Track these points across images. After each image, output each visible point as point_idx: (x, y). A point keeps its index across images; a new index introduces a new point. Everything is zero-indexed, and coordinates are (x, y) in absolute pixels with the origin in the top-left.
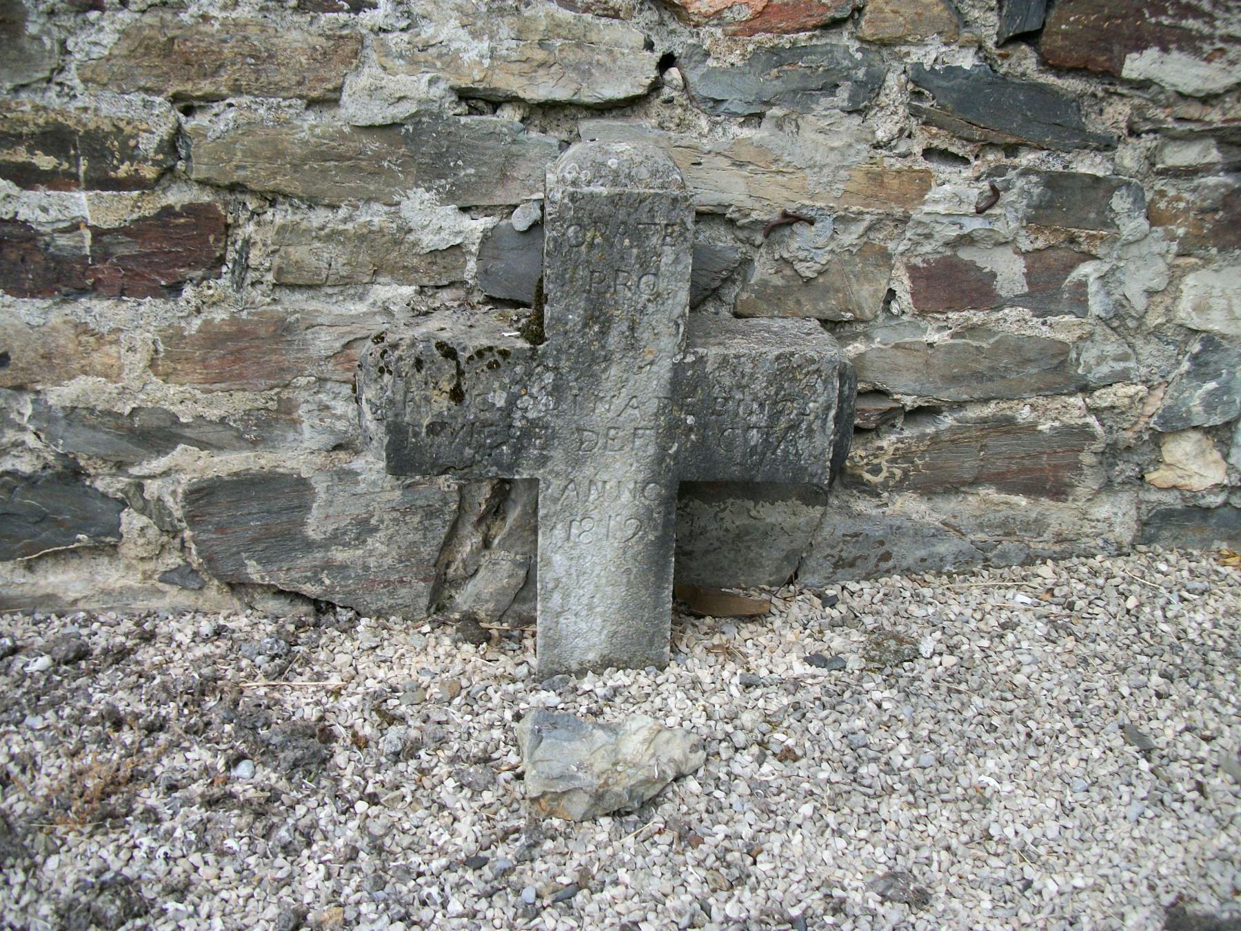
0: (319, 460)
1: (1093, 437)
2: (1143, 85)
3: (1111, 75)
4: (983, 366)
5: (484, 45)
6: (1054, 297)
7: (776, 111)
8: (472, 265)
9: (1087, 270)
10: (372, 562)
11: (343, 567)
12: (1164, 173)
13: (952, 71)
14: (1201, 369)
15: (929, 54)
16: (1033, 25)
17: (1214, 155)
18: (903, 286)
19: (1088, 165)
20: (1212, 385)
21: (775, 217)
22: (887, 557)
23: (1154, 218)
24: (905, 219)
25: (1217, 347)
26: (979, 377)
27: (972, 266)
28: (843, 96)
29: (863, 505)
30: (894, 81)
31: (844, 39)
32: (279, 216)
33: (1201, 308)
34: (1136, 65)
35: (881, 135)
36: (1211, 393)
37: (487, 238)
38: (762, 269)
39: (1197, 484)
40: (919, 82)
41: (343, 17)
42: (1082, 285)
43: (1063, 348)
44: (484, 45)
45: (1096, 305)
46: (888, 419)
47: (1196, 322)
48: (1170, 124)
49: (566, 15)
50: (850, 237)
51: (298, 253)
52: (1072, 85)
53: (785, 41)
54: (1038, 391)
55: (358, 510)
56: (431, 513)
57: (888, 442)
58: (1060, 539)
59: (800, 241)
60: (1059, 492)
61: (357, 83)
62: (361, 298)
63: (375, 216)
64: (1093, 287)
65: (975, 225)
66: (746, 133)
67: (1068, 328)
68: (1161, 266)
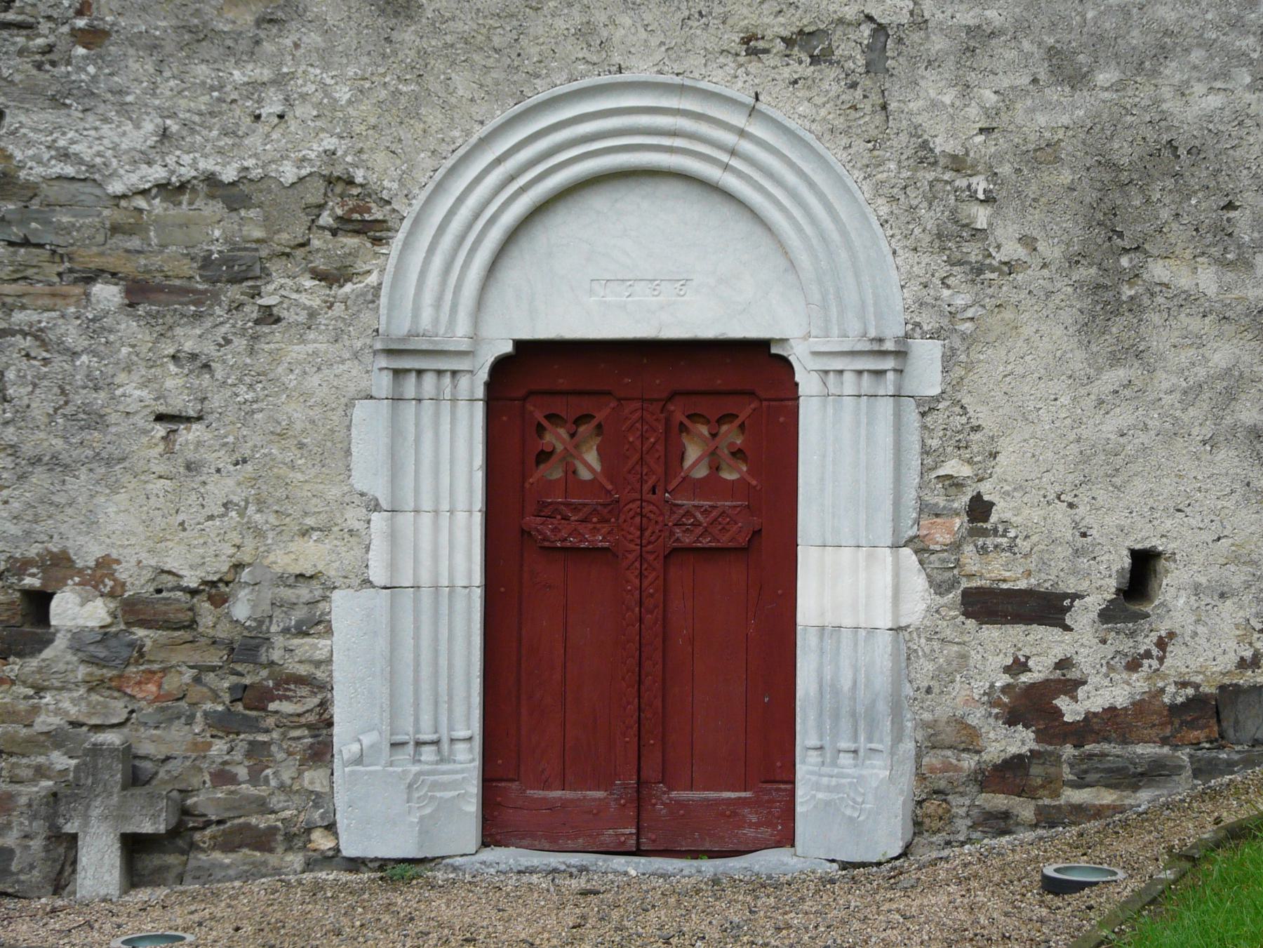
0: (18, 841)
1: (279, 829)
2: (276, 712)
3: (264, 709)
4: (236, 804)
5: (77, 708)
6: (258, 780)
7: (163, 725)
8: (72, 775)
9: (269, 771)
10: (33, 880)
11: (23, 882)
12: (290, 739)
13: (215, 711)
14: (317, 806)
15: (208, 706)
16: (239, 697)
17: (306, 732)
18: (207, 778)
19: (262, 738)
20: (322, 810)
21: (163, 757)
22: (210, 875)
23: (290, 754)
24: (205, 757)
25: (321, 797)
26: (235, 808)
27: (229, 772)
28: (183, 720)
29: (202, 856)
30: (198, 715)
31: (183, 704)
32: (14, 760)
33: (312, 783)
34: (273, 706)
35: (197, 731)
36: (322, 813)
37: (77, 767)
38: (162, 774)
39: (323, 847)
40: (206, 714)
41: (36, 701)
42: (267, 776)
43: (263, 798)
44: (77, 708)
45: (273, 783)
46: (208, 824)
47: (311, 788)
48: (288, 724)
49: (102, 699)
50: (188, 763)
51: (17, 771)
52: (254, 713)
53: (164, 704)
54: (257, 813)
55: (30, 860)
56: (54, 861)
57: (208, 832)
58: (274, 868)
59: (170, 765)
60: (271, 850)
61: (39, 720)
62: (36, 786)
63: (41, 759)
64: (271, 777)
65: (227, 758)
66: (155, 732)
67: (264, 791)
68: (294, 769)
